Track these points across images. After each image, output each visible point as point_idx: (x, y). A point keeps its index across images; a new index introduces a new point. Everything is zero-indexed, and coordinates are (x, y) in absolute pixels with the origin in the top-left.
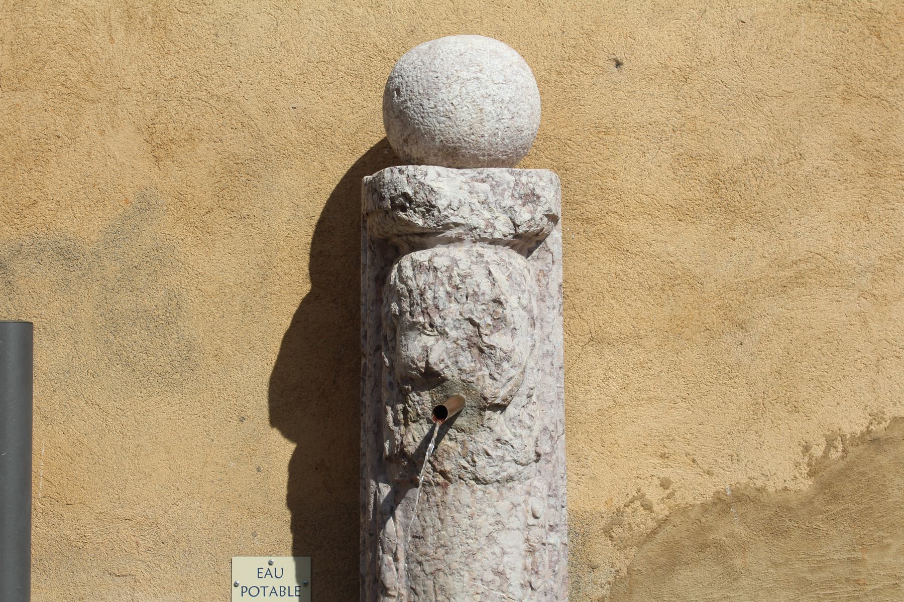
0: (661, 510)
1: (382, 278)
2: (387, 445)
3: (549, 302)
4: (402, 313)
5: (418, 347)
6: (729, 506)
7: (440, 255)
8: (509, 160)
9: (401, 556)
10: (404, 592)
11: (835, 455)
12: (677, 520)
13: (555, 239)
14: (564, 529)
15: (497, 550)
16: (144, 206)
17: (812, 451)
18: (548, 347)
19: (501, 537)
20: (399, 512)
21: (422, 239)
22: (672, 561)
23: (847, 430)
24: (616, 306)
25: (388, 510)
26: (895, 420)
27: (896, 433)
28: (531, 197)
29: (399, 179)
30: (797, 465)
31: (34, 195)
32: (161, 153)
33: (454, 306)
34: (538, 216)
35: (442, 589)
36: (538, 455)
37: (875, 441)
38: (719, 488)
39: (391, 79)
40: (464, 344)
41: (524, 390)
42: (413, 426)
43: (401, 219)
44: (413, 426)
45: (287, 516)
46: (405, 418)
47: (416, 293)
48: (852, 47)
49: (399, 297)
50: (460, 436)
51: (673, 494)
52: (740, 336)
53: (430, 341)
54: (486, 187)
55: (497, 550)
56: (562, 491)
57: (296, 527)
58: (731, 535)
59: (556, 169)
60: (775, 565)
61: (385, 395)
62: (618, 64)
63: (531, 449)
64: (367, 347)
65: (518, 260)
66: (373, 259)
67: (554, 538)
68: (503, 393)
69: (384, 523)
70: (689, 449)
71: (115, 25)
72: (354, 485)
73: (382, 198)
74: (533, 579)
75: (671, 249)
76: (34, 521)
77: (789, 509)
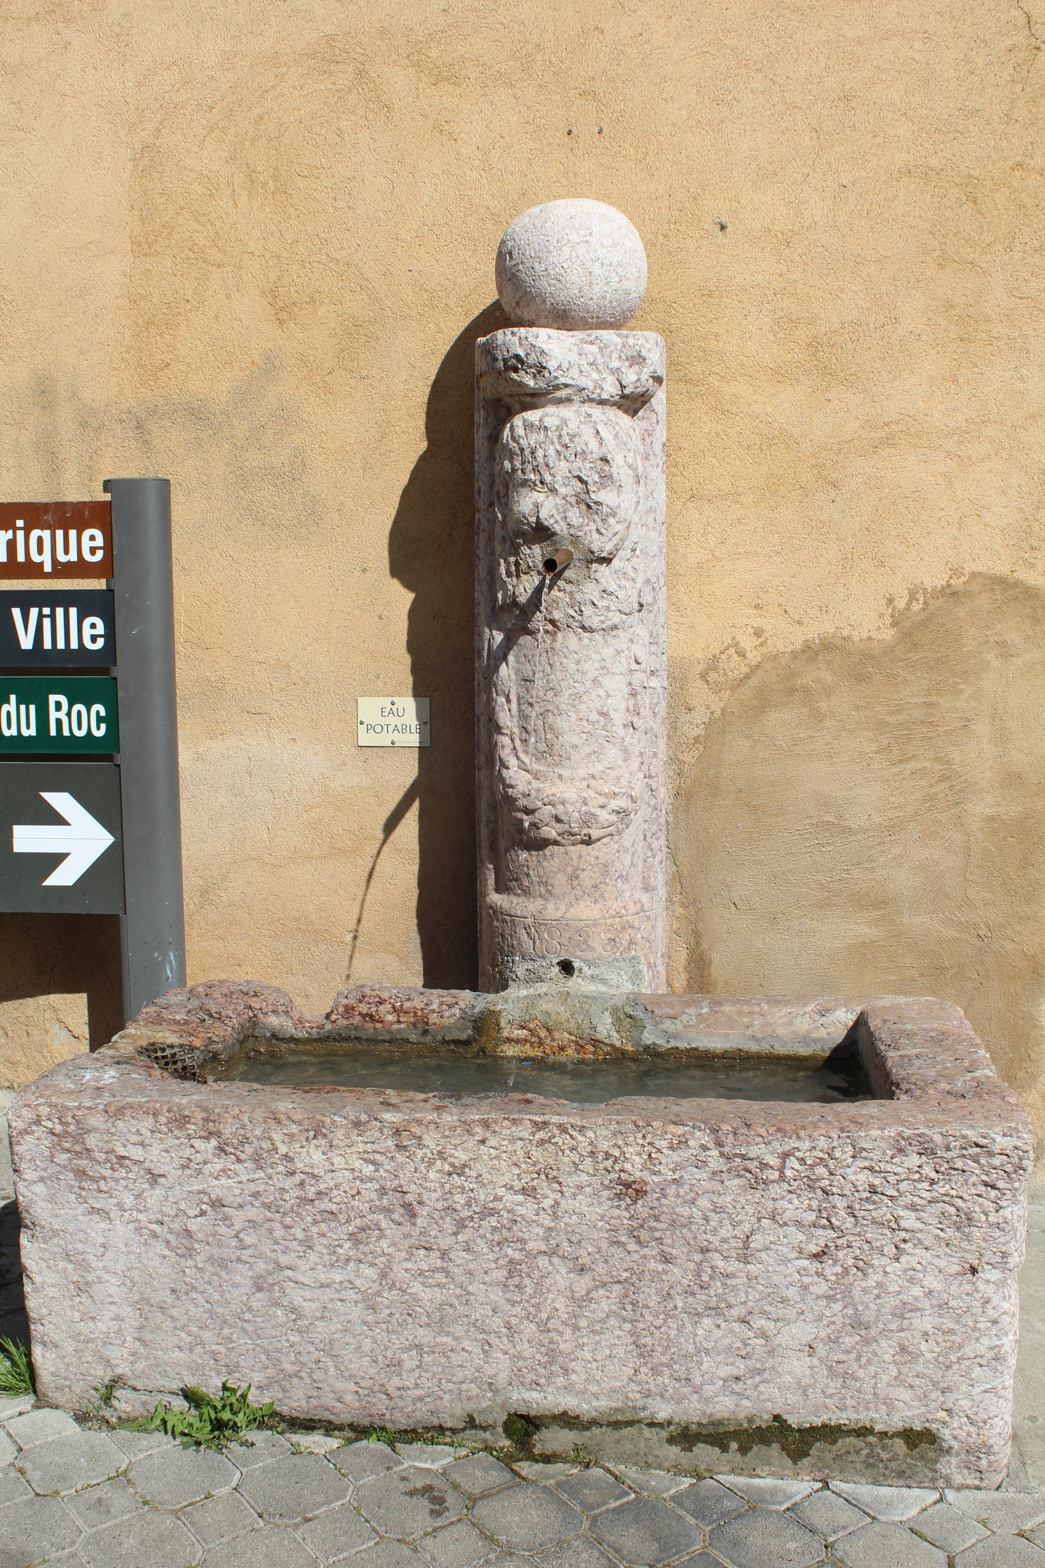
0: (754, 657)
1: (495, 437)
2: (500, 596)
3: (653, 460)
5: (529, 503)
6: (817, 654)
7: (549, 415)
8: (615, 323)
9: (513, 698)
10: (516, 730)
11: (916, 607)
12: (768, 666)
13: (660, 399)
14: (664, 674)
15: (602, 693)
17: (896, 603)
18: (652, 503)
19: (605, 681)
20: (511, 658)
21: (532, 399)
22: (762, 703)
23: (928, 584)
24: (717, 465)
26: (973, 575)
28: (637, 359)
29: (510, 340)
30: (881, 616)
31: (166, 357)
32: (284, 315)
33: (563, 464)
34: (644, 377)
35: (551, 728)
36: (641, 605)
38: (808, 637)
39: (503, 242)
40: (573, 500)
41: (628, 544)
42: (524, 577)
43: (513, 380)
44: (524, 577)
45: (408, 660)
46: (517, 570)
47: (527, 452)
49: (511, 455)
50: (568, 588)
51: (765, 642)
52: (833, 494)
53: (540, 497)
54: (594, 349)
55: (602, 693)
57: (415, 670)
58: (818, 680)
59: (661, 331)
60: (857, 708)
61: (498, 549)
63: (634, 600)
64: (481, 503)
65: (623, 419)
66: (486, 420)
67: (654, 683)
68: (609, 547)
69: (498, 667)
70: (781, 600)
71: (238, 189)
72: (469, 632)
73: (495, 360)
74: (635, 720)
75: (770, 410)
76: (178, 664)
77: (872, 657)
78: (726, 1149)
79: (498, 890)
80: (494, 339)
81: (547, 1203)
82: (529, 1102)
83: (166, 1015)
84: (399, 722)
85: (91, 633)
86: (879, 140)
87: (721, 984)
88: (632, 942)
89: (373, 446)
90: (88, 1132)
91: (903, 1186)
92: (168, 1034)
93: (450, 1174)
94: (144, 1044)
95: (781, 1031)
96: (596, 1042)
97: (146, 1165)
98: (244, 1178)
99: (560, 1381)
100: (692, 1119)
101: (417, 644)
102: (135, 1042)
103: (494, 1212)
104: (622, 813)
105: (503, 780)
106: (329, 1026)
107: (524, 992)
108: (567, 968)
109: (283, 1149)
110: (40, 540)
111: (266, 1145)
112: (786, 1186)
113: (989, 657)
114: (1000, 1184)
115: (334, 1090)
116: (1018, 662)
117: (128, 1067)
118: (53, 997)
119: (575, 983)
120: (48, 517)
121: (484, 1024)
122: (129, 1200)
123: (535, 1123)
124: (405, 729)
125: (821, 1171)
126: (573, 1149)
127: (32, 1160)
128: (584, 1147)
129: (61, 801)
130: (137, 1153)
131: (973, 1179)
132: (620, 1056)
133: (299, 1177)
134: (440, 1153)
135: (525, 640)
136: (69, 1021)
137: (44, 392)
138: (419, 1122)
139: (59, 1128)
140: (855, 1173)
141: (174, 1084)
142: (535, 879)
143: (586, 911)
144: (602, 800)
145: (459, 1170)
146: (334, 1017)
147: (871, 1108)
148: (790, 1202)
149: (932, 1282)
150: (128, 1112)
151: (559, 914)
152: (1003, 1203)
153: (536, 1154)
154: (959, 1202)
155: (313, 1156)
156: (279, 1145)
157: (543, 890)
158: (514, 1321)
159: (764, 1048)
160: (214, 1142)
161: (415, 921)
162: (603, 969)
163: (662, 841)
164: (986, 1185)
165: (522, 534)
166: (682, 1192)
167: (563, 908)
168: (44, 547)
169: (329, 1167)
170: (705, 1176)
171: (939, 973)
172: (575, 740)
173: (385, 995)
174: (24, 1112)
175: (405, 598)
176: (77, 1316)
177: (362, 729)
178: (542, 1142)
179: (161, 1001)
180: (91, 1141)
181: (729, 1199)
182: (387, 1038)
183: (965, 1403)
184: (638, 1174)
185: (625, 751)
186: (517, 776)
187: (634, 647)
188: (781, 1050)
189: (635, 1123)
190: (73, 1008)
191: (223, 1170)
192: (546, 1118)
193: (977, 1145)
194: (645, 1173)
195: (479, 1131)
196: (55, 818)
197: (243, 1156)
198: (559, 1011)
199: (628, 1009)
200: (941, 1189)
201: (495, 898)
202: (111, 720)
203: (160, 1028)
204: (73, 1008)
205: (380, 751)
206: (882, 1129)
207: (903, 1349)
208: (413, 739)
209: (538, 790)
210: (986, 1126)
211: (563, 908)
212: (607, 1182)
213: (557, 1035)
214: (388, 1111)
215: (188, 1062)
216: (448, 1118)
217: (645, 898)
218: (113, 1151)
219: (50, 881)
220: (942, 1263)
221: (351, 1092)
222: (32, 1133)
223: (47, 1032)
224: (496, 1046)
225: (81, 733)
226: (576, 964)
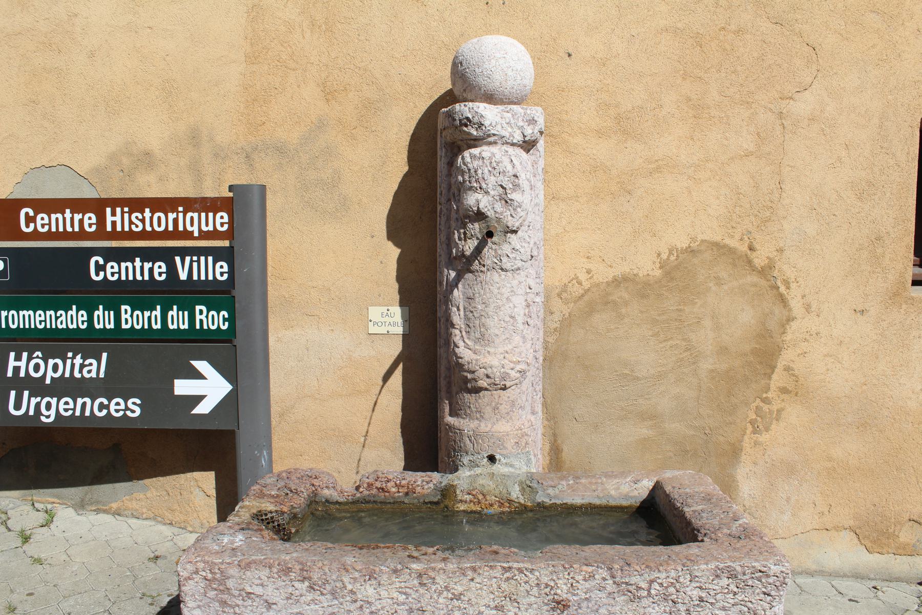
0: (586, 285)
1: (451, 163)
2: (454, 251)
3: (538, 178)
4: (464, 181)
5: (472, 200)
6: (620, 283)
7: (484, 151)
8: (518, 101)
9: (461, 308)
10: (463, 326)
11: (673, 258)
12: (594, 290)
13: (541, 145)
15: (511, 305)
16: (321, 125)
18: (537, 201)
19: (513, 299)
20: (460, 286)
21: (474, 142)
22: (591, 310)
23: (679, 246)
25: (455, 284)
26: (703, 241)
27: (703, 248)
28: (532, 122)
29: (463, 109)
30: (654, 262)
31: (263, 119)
32: (329, 97)
33: (492, 178)
34: (536, 131)
35: (483, 325)
39: (456, 57)
40: (498, 198)
41: (526, 223)
42: (469, 241)
43: (465, 132)
44: (469, 241)
45: (397, 286)
46: (465, 237)
47: (472, 171)
48: (687, 52)
49: (463, 173)
50: (494, 247)
52: (628, 197)
53: (480, 196)
54: (509, 115)
55: (511, 305)
56: (542, 275)
58: (621, 297)
60: (642, 312)
61: (453, 224)
62: (570, 55)
63: (529, 253)
64: (441, 199)
65: (523, 154)
66: (446, 153)
67: (538, 299)
68: (517, 224)
70: (601, 254)
71: (305, 29)
72: (433, 270)
73: (454, 120)
75: (595, 152)
76: (269, 288)
77: (650, 285)
78: (617, 579)
79: (451, 415)
80: (454, 109)
82: (496, 553)
83: (265, 491)
84: (391, 320)
85: (220, 271)
86: (651, 13)
87: (568, 462)
88: (527, 443)
89: (382, 167)
90: (228, 578)
91: (719, 597)
92: (268, 504)
93: (452, 599)
94: (255, 511)
95: (613, 493)
96: (510, 501)
97: (264, 597)
98: (325, 605)
100: (596, 562)
101: (401, 278)
102: (249, 510)
104: (522, 372)
105: (456, 354)
106: (358, 495)
107: (468, 473)
108: (492, 459)
109: (349, 587)
110: (192, 218)
111: (339, 584)
112: (651, 600)
113: (711, 285)
114: (773, 593)
115: (377, 547)
116: (725, 287)
117: (250, 532)
118: (195, 473)
119: (497, 468)
120: (197, 206)
121: (447, 492)
123: (504, 568)
124: (395, 324)
125: (672, 590)
126: (526, 582)
127: (193, 595)
128: (533, 581)
129: (202, 366)
130: (258, 590)
131: (758, 591)
132: (524, 509)
133: (359, 604)
134: (446, 587)
135: (469, 276)
136: (204, 487)
137: (194, 138)
138: (434, 569)
139: (210, 576)
140: (691, 590)
141: (279, 545)
142: (474, 410)
143: (502, 427)
144: (512, 365)
145: (458, 597)
146: (361, 490)
147: (692, 549)
148: (653, 609)
150: (253, 566)
151: (488, 429)
152: (774, 604)
153: (504, 586)
154: (750, 605)
155: (368, 591)
156: (347, 584)
157: (478, 416)
159: (603, 502)
160: (307, 584)
161: (400, 430)
162: (512, 459)
163: (541, 387)
164: (765, 593)
165: (469, 217)
166: (590, 605)
167: (490, 426)
168: (194, 222)
169: (377, 597)
170: (604, 595)
171: (685, 453)
172: (497, 332)
173: (391, 477)
174: (188, 566)
175: (396, 252)
177: (371, 324)
178: (508, 579)
179: (262, 481)
180: (230, 583)
181: (618, 608)
182: (392, 501)
184: (565, 596)
185: (524, 337)
186: (465, 352)
187: (528, 280)
188: (613, 503)
189: (563, 566)
190: (207, 480)
191: (312, 600)
192: (510, 564)
193: (760, 571)
194: (569, 595)
195: (470, 574)
196: (199, 376)
197: (325, 592)
198: (489, 485)
199: (528, 482)
200: (740, 597)
201: (449, 419)
202: (231, 320)
203: (262, 501)
204: (207, 480)
205: (381, 337)
206: (707, 564)
208: (400, 330)
209: (477, 360)
210: (764, 560)
211: (490, 426)
212: (546, 601)
213: (488, 498)
214: (414, 562)
215: (281, 522)
216: (451, 566)
217: (532, 418)
218: (244, 589)
219: (195, 411)
221: (388, 547)
222: (193, 579)
223: (192, 493)
224: (454, 504)
225: (215, 327)
226: (497, 457)
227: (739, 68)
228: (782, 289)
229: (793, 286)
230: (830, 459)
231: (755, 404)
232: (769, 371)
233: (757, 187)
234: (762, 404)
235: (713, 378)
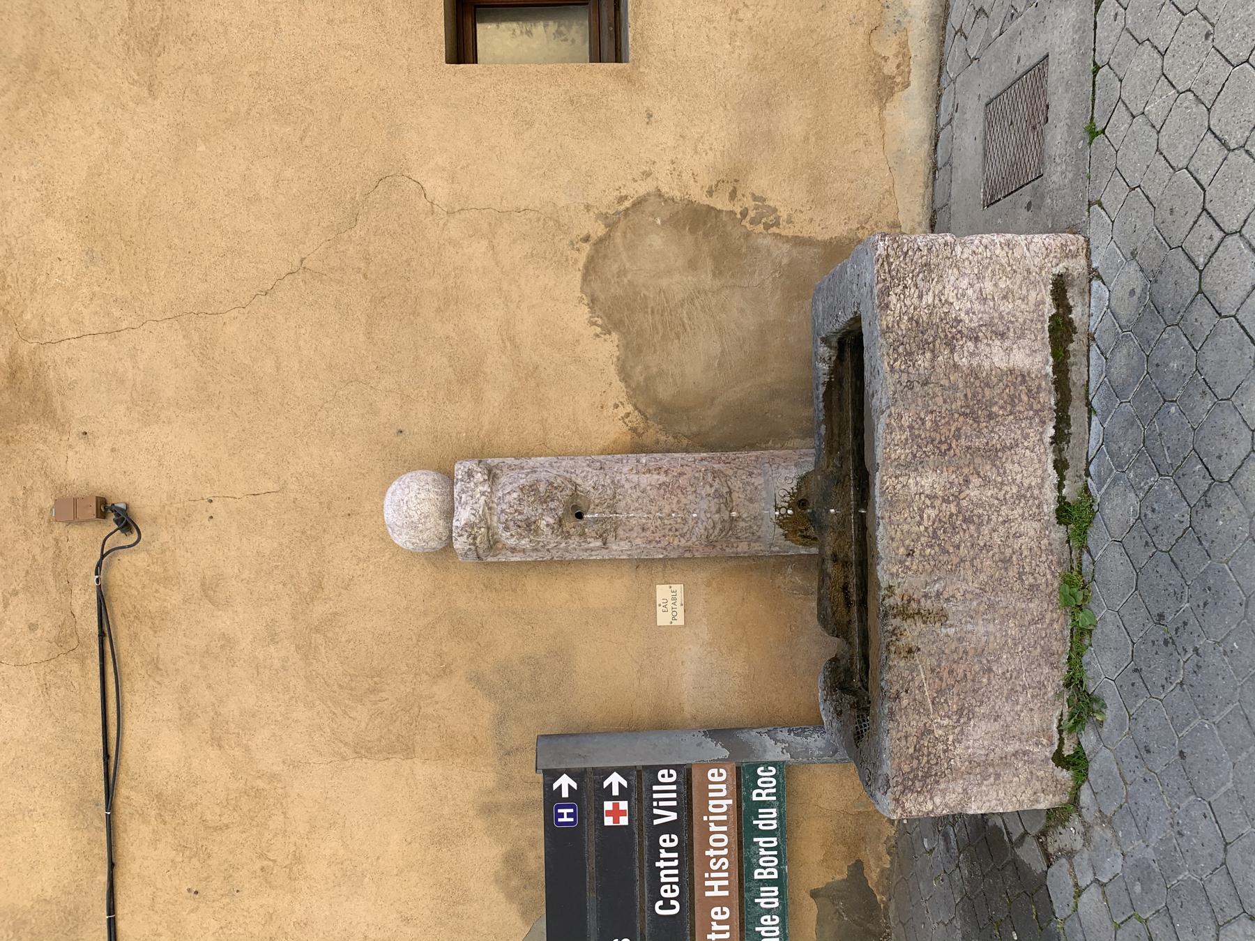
0: (630, 408)
11: (600, 321)
16: (476, 679)
19: (643, 486)
26: (582, 292)
37: (593, 301)
41: (568, 476)
58: (641, 373)
60: (655, 351)
63: (598, 472)
81: (928, 502)
91: (908, 302)
99: (1036, 492)
103: (934, 532)
116: (628, 265)
122: (941, 747)
125: (901, 350)
139: (900, 788)
145: (910, 553)
149: (964, 283)
158: (1001, 519)
176: (1016, 779)
177: (675, 623)
183: (1037, 261)
207: (1005, 297)
220: (953, 278)
227: (404, 258)
228: (627, 204)
229: (624, 192)
230: (806, 139)
231: (748, 225)
232: (713, 213)
233: (524, 236)
234: (748, 218)
235: (720, 273)
